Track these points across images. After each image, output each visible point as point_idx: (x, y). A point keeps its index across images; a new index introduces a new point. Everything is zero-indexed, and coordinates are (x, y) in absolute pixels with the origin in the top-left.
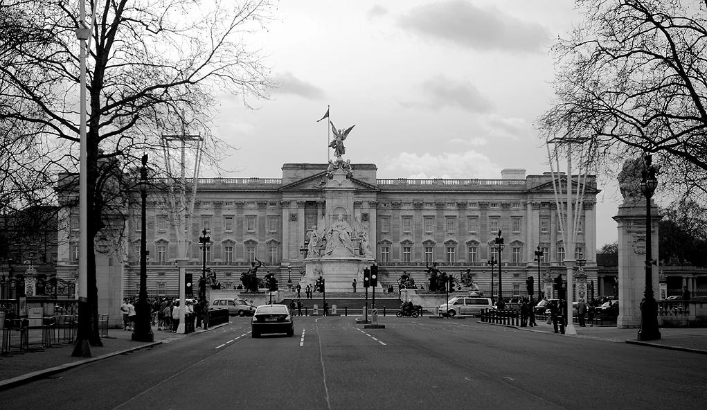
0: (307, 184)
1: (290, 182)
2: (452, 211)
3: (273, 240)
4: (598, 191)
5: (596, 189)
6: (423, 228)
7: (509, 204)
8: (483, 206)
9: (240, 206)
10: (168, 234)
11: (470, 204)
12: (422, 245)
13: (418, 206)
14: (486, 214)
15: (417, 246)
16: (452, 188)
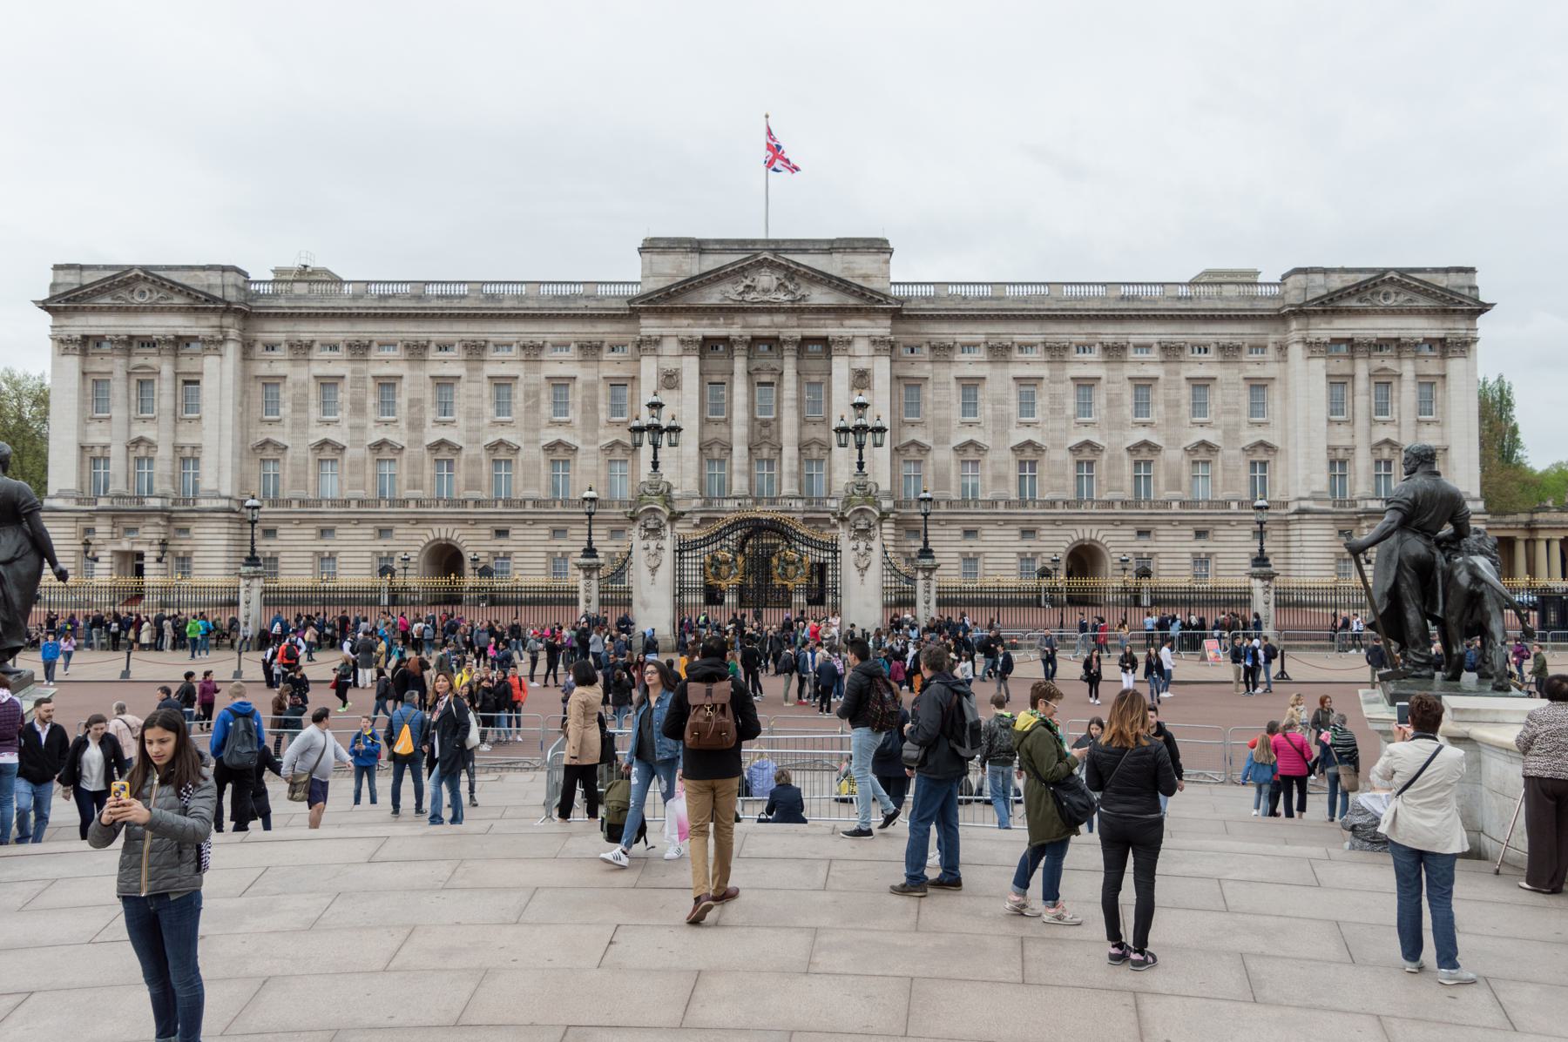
0: (706, 291)
1: (661, 285)
2: (1090, 365)
3: (617, 443)
4: (1484, 308)
5: (1476, 300)
6: (1013, 408)
7: (1239, 348)
8: (1171, 352)
9: (532, 351)
10: (345, 425)
11: (1137, 346)
12: (1011, 456)
13: (999, 353)
14: (1178, 374)
15: (1001, 460)
16: (1089, 305)
